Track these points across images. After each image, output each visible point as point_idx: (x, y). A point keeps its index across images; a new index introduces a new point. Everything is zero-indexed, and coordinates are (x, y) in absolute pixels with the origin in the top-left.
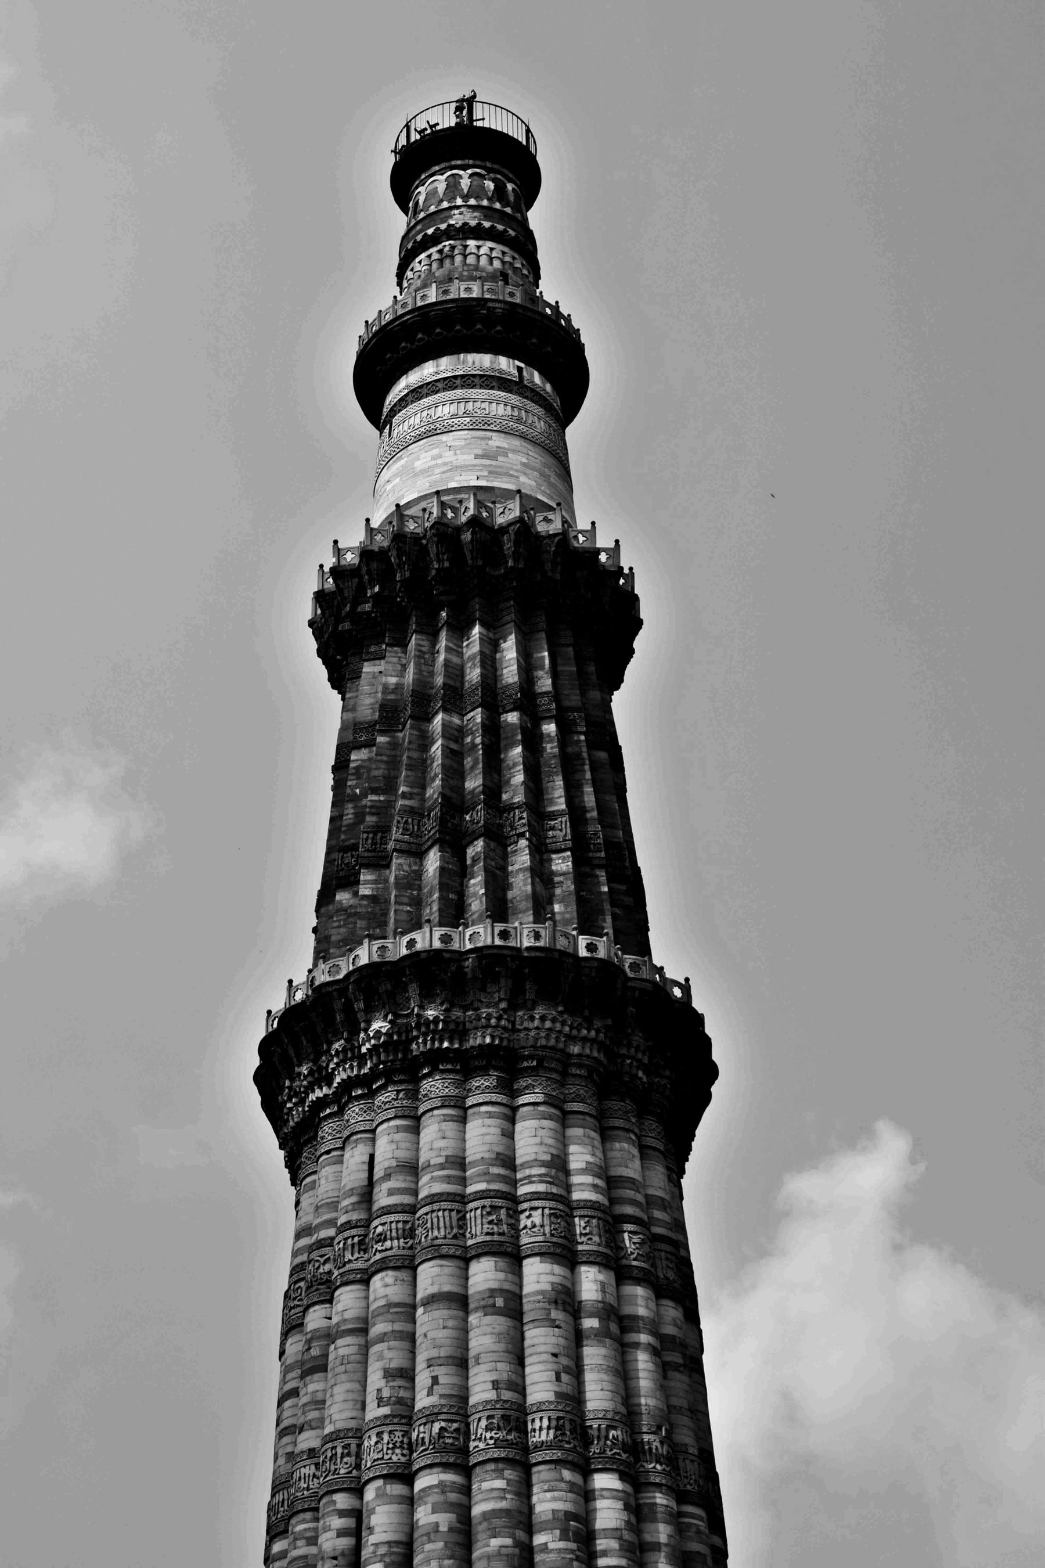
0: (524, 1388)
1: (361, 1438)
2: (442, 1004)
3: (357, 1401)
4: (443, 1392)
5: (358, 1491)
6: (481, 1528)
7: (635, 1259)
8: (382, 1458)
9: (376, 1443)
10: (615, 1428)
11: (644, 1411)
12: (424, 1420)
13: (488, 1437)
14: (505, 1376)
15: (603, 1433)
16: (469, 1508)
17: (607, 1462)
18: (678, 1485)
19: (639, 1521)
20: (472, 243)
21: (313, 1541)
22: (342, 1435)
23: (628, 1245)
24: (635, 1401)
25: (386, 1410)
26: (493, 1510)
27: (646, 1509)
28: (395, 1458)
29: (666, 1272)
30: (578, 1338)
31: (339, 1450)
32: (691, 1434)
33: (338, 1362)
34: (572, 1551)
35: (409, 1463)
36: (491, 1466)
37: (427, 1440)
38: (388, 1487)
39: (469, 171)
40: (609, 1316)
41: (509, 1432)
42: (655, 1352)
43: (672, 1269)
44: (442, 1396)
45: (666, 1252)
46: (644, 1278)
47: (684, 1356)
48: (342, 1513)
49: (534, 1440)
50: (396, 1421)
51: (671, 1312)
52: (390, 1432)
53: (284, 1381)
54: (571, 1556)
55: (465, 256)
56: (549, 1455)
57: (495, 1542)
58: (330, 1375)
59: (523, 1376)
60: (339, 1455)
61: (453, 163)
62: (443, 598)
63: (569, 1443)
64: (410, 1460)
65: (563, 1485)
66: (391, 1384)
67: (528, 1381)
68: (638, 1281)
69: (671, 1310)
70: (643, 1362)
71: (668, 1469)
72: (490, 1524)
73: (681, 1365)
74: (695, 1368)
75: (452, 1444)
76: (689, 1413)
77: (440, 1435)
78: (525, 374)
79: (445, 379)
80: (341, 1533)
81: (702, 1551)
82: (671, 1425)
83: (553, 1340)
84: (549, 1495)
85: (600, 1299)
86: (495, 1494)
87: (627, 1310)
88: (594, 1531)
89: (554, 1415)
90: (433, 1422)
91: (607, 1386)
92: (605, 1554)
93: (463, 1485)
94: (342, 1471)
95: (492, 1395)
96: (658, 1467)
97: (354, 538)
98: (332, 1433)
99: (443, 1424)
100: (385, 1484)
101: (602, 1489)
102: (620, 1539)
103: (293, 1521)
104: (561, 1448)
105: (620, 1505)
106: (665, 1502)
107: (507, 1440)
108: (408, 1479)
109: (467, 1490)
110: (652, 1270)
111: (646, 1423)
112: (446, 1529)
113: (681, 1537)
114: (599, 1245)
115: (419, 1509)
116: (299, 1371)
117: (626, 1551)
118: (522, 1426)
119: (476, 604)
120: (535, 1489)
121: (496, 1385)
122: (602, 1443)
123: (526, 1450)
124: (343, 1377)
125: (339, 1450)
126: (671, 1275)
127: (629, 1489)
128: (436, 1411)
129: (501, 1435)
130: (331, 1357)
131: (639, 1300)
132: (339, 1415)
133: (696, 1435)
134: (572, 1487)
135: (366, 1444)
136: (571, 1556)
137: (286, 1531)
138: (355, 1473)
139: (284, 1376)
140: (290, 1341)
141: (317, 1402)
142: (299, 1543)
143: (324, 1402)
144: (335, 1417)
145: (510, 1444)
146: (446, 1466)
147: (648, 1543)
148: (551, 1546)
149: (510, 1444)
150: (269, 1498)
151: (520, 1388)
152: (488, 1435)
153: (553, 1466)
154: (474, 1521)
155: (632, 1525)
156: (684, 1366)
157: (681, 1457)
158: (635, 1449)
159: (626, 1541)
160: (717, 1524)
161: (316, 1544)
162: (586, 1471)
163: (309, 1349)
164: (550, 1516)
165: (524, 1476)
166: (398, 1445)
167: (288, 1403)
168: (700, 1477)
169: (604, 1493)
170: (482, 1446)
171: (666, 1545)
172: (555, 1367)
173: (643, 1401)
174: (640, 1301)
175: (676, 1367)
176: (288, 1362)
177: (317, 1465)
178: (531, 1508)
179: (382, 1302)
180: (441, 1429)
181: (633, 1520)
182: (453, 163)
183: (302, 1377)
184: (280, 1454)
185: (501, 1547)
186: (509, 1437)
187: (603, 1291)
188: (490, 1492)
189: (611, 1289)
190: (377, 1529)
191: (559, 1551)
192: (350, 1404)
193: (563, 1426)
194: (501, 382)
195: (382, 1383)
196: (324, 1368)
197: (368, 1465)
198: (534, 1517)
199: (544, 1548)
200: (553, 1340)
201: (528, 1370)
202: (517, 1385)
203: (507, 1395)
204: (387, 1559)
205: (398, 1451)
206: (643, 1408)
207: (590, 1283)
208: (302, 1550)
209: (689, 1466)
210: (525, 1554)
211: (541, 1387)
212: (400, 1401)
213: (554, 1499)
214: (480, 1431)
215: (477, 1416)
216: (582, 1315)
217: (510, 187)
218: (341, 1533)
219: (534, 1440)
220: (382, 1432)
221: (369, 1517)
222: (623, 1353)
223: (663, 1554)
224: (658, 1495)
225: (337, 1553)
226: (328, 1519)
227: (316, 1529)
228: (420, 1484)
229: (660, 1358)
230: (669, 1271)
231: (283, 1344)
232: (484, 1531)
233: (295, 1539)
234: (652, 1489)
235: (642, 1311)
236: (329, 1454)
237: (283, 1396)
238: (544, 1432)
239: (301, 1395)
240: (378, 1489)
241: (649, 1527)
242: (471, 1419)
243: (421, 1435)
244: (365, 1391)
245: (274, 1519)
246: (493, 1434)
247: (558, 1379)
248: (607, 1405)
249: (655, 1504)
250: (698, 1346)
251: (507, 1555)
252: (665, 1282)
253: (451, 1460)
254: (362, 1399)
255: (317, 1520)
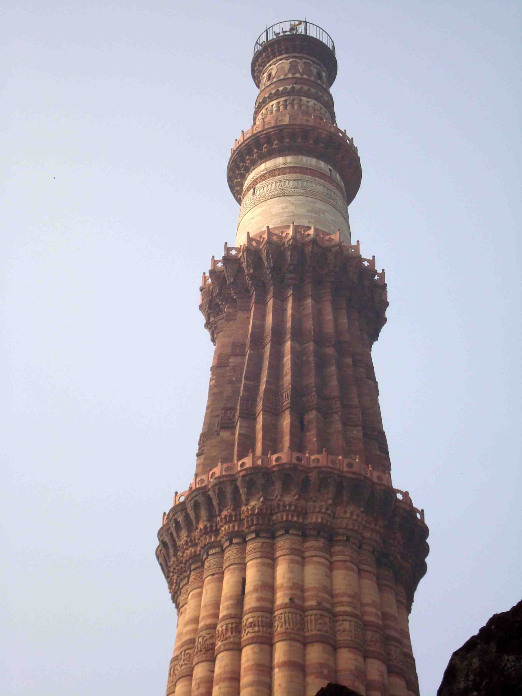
2: (294, 496)
20: (304, 99)
39: (304, 60)
55: (301, 105)
61: (294, 54)
62: (289, 281)
78: (333, 173)
79: (290, 168)
97: (239, 241)
119: (309, 288)
182: (294, 54)
194: (321, 175)
217: (324, 74)
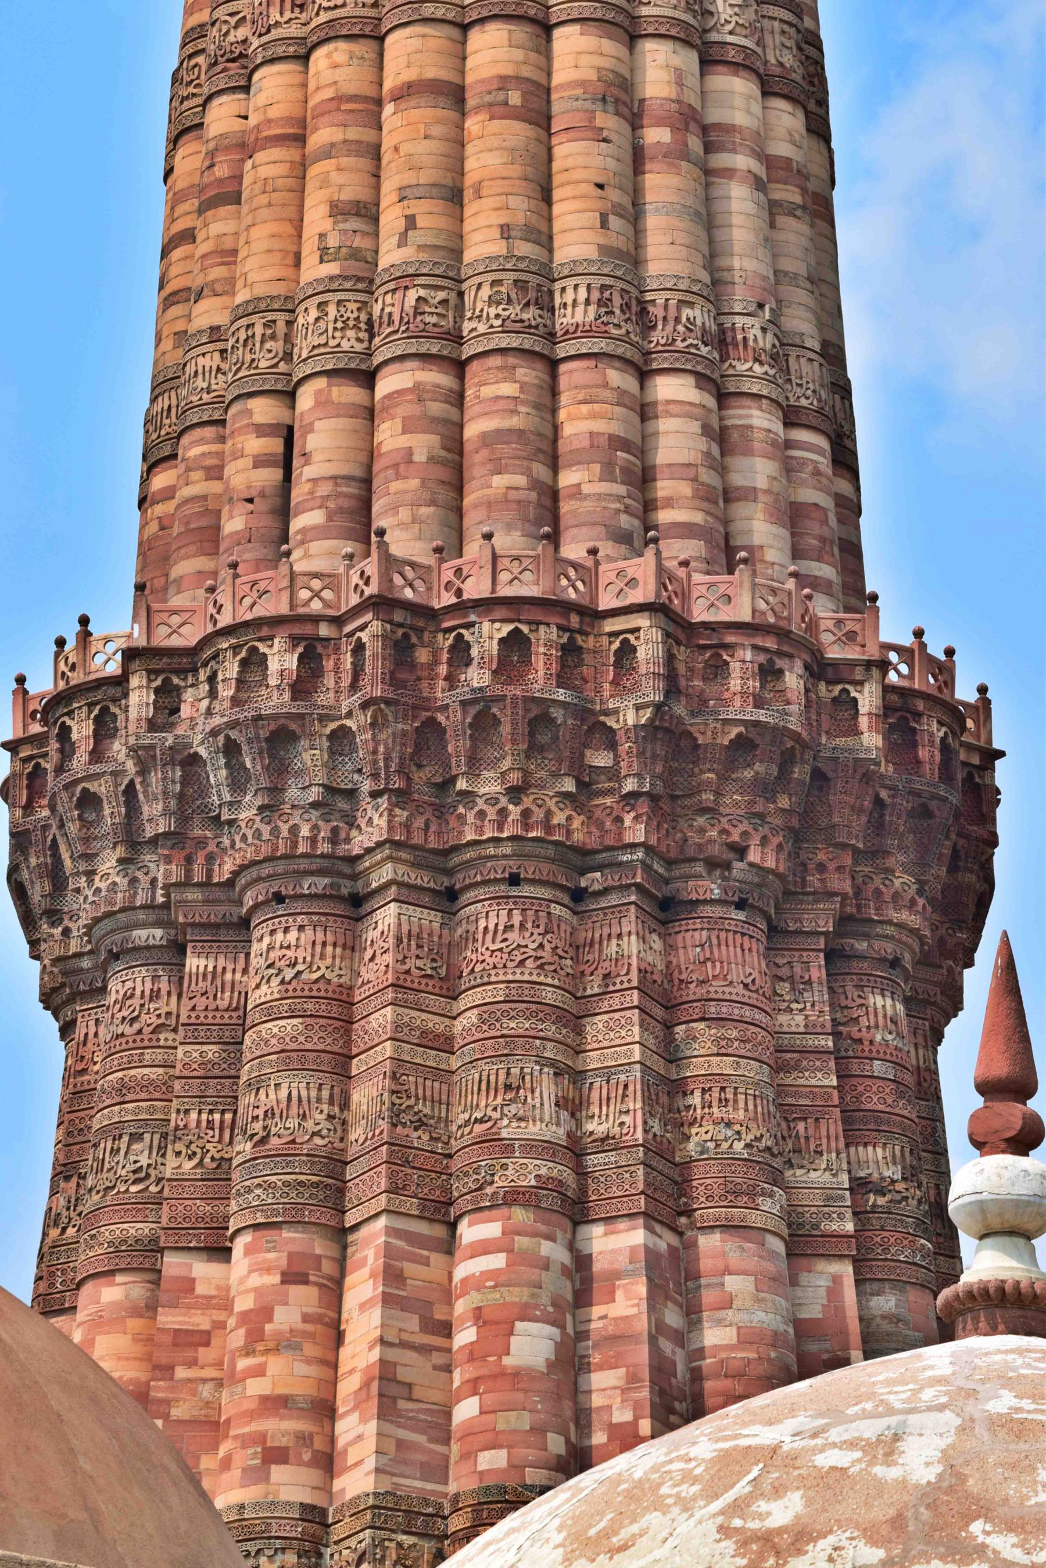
0: (551, 238)
1: (293, 311)
3: (287, 252)
4: (422, 241)
5: (290, 396)
6: (478, 458)
7: (731, 33)
8: (326, 344)
9: (317, 320)
10: (691, 304)
11: (737, 280)
12: (392, 285)
13: (492, 315)
14: (520, 219)
15: (672, 313)
16: (461, 427)
17: (677, 359)
18: (787, 398)
19: (722, 455)
21: (215, 473)
22: (263, 306)
23: (721, 9)
24: (723, 262)
25: (332, 268)
26: (498, 431)
27: (735, 436)
28: (346, 345)
29: (780, 54)
30: (638, 158)
31: (259, 330)
32: (809, 315)
33: (258, 187)
34: (619, 498)
35: (369, 354)
36: (496, 361)
37: (396, 318)
38: (335, 390)
40: (687, 125)
41: (527, 305)
42: (760, 185)
43: (790, 48)
44: (420, 247)
45: (781, 20)
46: (745, 64)
47: (804, 191)
48: (261, 430)
49: (565, 320)
50: (348, 285)
51: (787, 119)
52: (339, 303)
53: (171, 218)
54: (617, 505)
56: (586, 346)
57: (499, 481)
58: (245, 208)
59: (550, 220)
60: (258, 338)
63: (618, 326)
64: (369, 348)
65: (607, 394)
66: (341, 226)
67: (557, 226)
68: (735, 67)
69: (785, 116)
70: (739, 201)
71: (772, 372)
72: (492, 452)
73: (799, 206)
74: (820, 210)
75: (434, 325)
76: (809, 286)
77: (417, 312)
80: (259, 462)
81: (822, 504)
82: (779, 302)
83: (598, 162)
84: (585, 408)
85: (674, 96)
86: (502, 405)
87: (713, 116)
88: (654, 466)
89: (597, 282)
90: (406, 288)
91: (682, 238)
92: (670, 503)
93: (451, 390)
94: (263, 364)
95: (499, 248)
96: (757, 368)
98: (248, 302)
99: (422, 292)
100: (329, 385)
101: (669, 402)
102: (695, 480)
103: (185, 440)
104: (605, 335)
105: (696, 427)
106: (766, 424)
107: (522, 321)
108: (368, 378)
109: (458, 399)
110: (759, 50)
111: (740, 298)
112: (424, 459)
113: (789, 480)
114: (675, 7)
115: (383, 426)
116: (196, 202)
117: (702, 499)
118: (546, 298)
120: (564, 399)
121: (506, 232)
122: (670, 328)
123: (551, 336)
124: (264, 213)
125: (259, 330)
126: (788, 59)
127: (711, 402)
128: (411, 271)
129: (514, 311)
130: (247, 181)
131: (735, 98)
132: (258, 275)
133: (818, 319)
134: (622, 398)
135: (301, 320)
136: (617, 505)
137: (174, 456)
138: (283, 367)
139: (172, 208)
140: (180, 153)
141: (223, 253)
142: (196, 475)
143: (235, 252)
144: (252, 277)
145: (528, 328)
146: (425, 358)
147: (737, 489)
148: (586, 489)
149: (528, 328)
150: (147, 405)
151: (546, 241)
152: (493, 311)
153: (592, 363)
154: (468, 447)
155: (714, 459)
156: (804, 207)
157: (793, 353)
158: (723, 341)
159: (702, 484)
160: (845, 459)
161: (220, 478)
162: (644, 375)
163: (212, 166)
164: (586, 443)
165: (547, 378)
166: (351, 323)
167: (177, 254)
168: (822, 386)
169: (671, 407)
170: (482, 328)
171: (767, 492)
172: (599, 205)
173: (736, 263)
174: (738, 102)
175: (791, 211)
176: (180, 185)
177: (223, 352)
178: (556, 428)
179: (328, 93)
180: (419, 299)
181: (716, 451)
183: (200, 211)
184: (165, 334)
185: (509, 488)
186: (525, 316)
187: (680, 84)
188: (496, 398)
189: (693, 80)
190: (316, 457)
191: (599, 496)
192: (277, 258)
193: (610, 300)
195: (327, 225)
196: (235, 198)
197: (304, 355)
198: (560, 442)
199: (576, 492)
200: (598, 162)
201: (556, 209)
202: (540, 232)
203: (524, 248)
204: (331, 505)
205: (351, 333)
206: (737, 274)
207: (660, 69)
208: (198, 486)
209: (806, 368)
210: (547, 502)
211: (576, 239)
212: (355, 254)
213: (593, 416)
214: (479, 306)
215: (476, 280)
216: (645, 122)
218: (259, 462)
219: (565, 320)
220: (326, 303)
221: (304, 436)
222: (708, 185)
223: (760, 506)
224: (756, 412)
225: (253, 493)
226: (241, 438)
227: (220, 455)
228: (385, 386)
229: (766, 195)
230: (785, 51)
231: (170, 155)
232: (483, 464)
233: (188, 470)
234: (747, 402)
235: (740, 119)
236: (242, 335)
237: (170, 241)
238: (580, 309)
239: (198, 240)
240: (318, 393)
241: (737, 462)
242: (465, 286)
243: (388, 310)
244: (300, 237)
245: (154, 436)
246: (499, 310)
247: (604, 224)
248: (681, 268)
249: (751, 427)
250: (826, 176)
251: (519, 502)
252: (778, 71)
253: (434, 350)
254: (294, 248)
255: (222, 439)
